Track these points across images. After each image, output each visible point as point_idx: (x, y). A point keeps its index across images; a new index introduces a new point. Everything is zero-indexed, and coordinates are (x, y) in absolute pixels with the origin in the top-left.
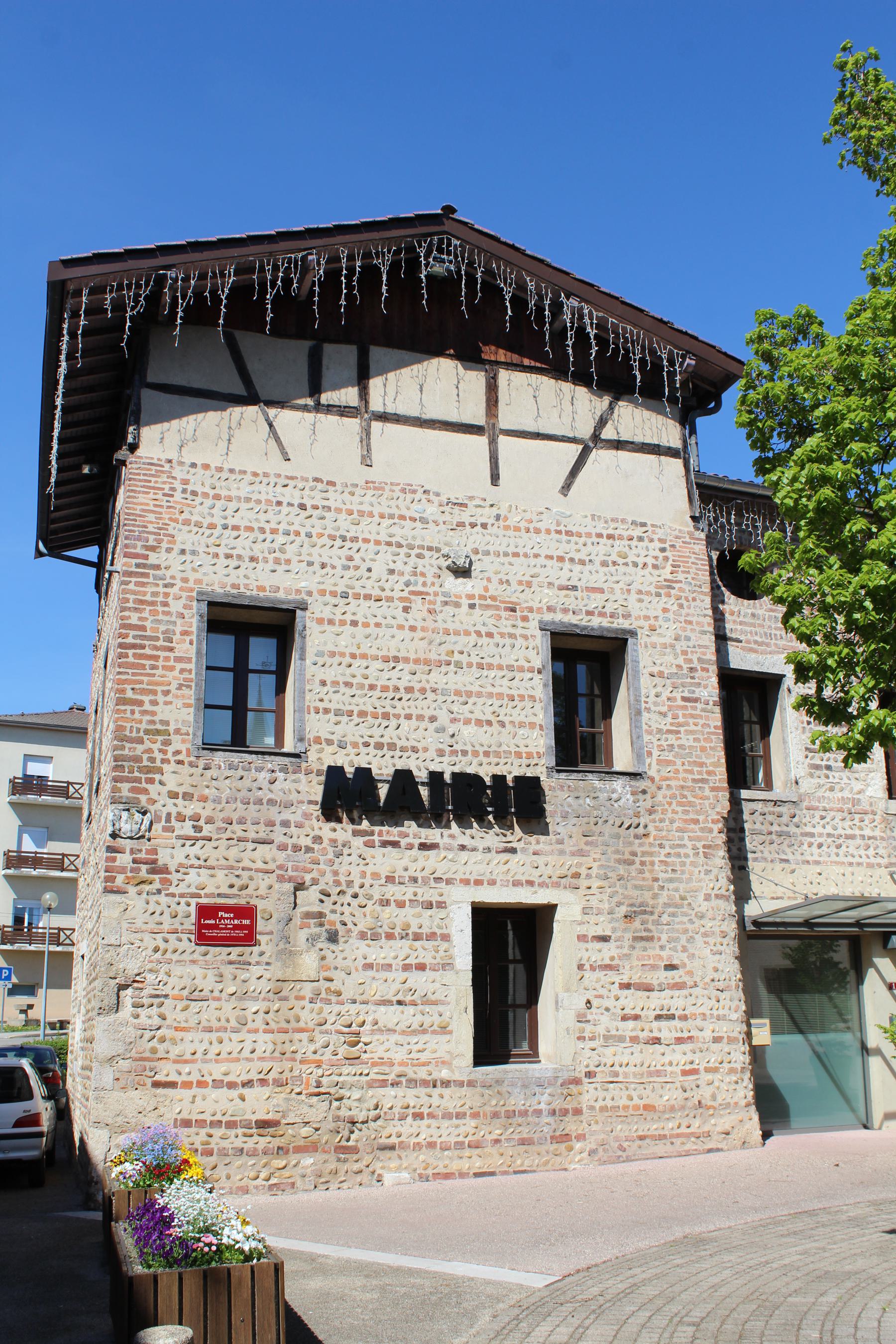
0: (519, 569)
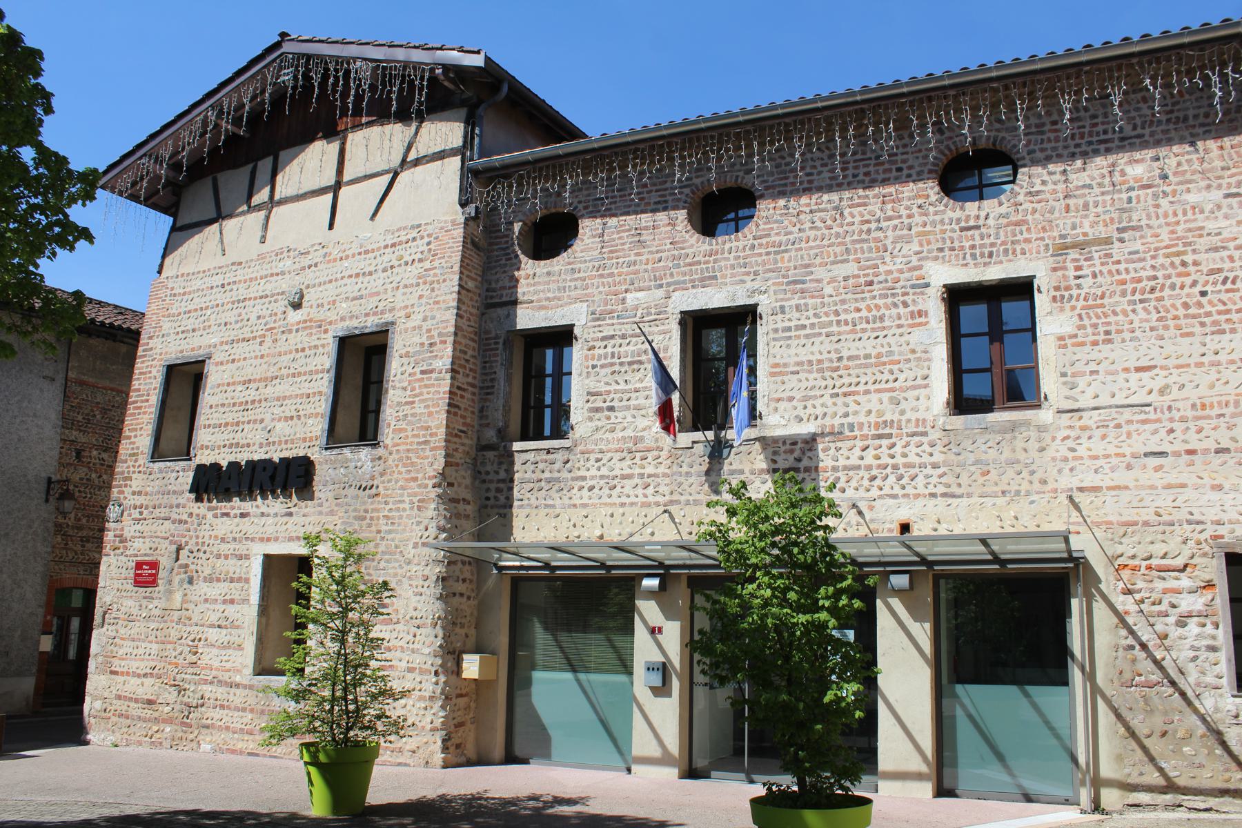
0: (330, 292)
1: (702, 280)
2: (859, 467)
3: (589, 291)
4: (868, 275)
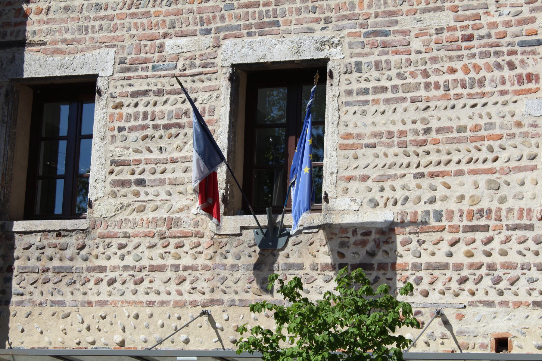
1: (261, 26)
2: (446, 266)
3: (119, 33)
4: (467, 27)
